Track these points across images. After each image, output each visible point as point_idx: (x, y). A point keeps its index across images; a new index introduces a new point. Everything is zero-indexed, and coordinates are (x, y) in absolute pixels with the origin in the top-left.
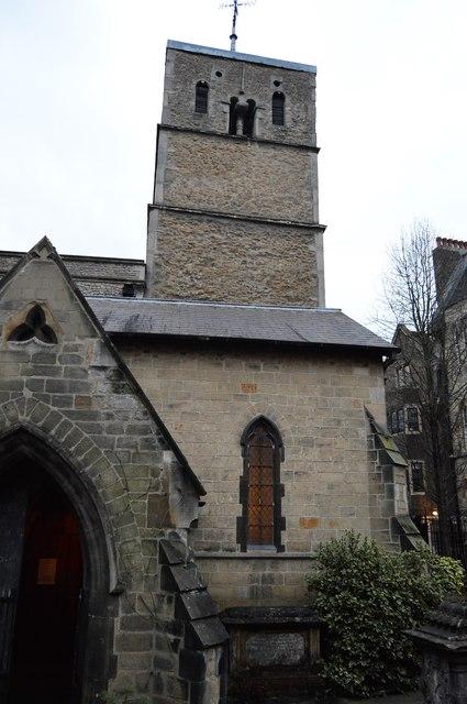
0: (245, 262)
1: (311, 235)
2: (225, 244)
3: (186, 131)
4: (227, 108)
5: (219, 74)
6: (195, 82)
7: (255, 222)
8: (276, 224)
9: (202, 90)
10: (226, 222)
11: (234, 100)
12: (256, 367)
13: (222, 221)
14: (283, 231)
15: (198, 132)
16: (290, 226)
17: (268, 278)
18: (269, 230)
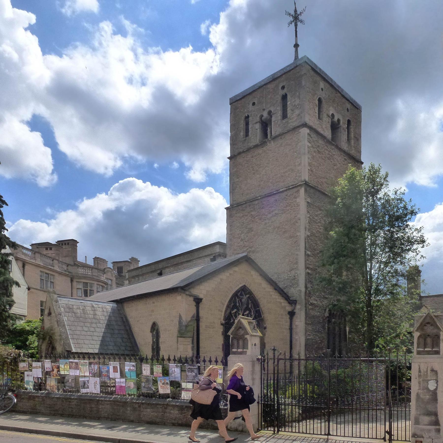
0: (266, 224)
1: (298, 191)
2: (257, 216)
3: (240, 153)
4: (258, 126)
5: (254, 104)
6: (243, 118)
7: (268, 196)
8: (278, 192)
9: (247, 117)
10: (257, 202)
11: (262, 116)
12: (154, 303)
13: (254, 203)
14: (283, 195)
15: (243, 152)
16: (286, 190)
17: (276, 229)
18: (277, 197)
